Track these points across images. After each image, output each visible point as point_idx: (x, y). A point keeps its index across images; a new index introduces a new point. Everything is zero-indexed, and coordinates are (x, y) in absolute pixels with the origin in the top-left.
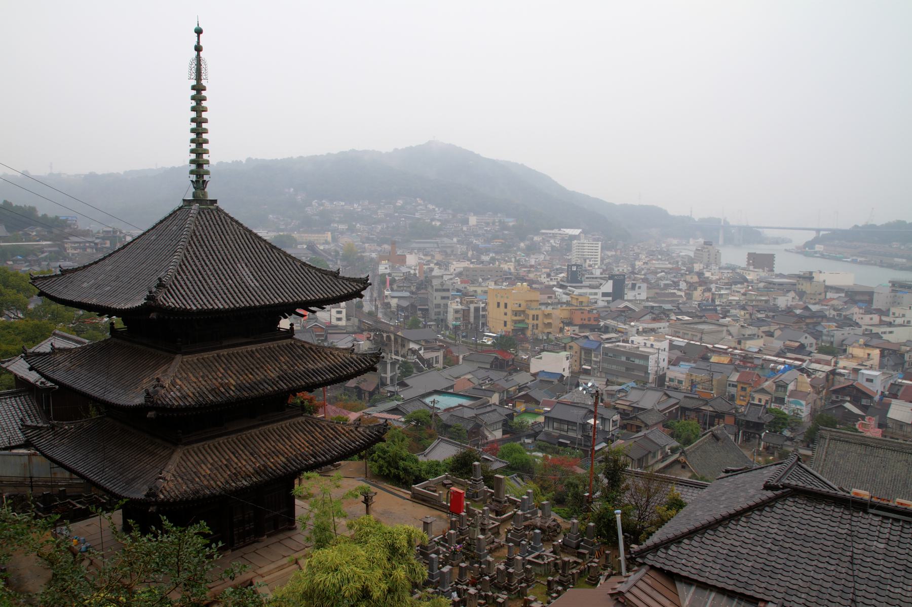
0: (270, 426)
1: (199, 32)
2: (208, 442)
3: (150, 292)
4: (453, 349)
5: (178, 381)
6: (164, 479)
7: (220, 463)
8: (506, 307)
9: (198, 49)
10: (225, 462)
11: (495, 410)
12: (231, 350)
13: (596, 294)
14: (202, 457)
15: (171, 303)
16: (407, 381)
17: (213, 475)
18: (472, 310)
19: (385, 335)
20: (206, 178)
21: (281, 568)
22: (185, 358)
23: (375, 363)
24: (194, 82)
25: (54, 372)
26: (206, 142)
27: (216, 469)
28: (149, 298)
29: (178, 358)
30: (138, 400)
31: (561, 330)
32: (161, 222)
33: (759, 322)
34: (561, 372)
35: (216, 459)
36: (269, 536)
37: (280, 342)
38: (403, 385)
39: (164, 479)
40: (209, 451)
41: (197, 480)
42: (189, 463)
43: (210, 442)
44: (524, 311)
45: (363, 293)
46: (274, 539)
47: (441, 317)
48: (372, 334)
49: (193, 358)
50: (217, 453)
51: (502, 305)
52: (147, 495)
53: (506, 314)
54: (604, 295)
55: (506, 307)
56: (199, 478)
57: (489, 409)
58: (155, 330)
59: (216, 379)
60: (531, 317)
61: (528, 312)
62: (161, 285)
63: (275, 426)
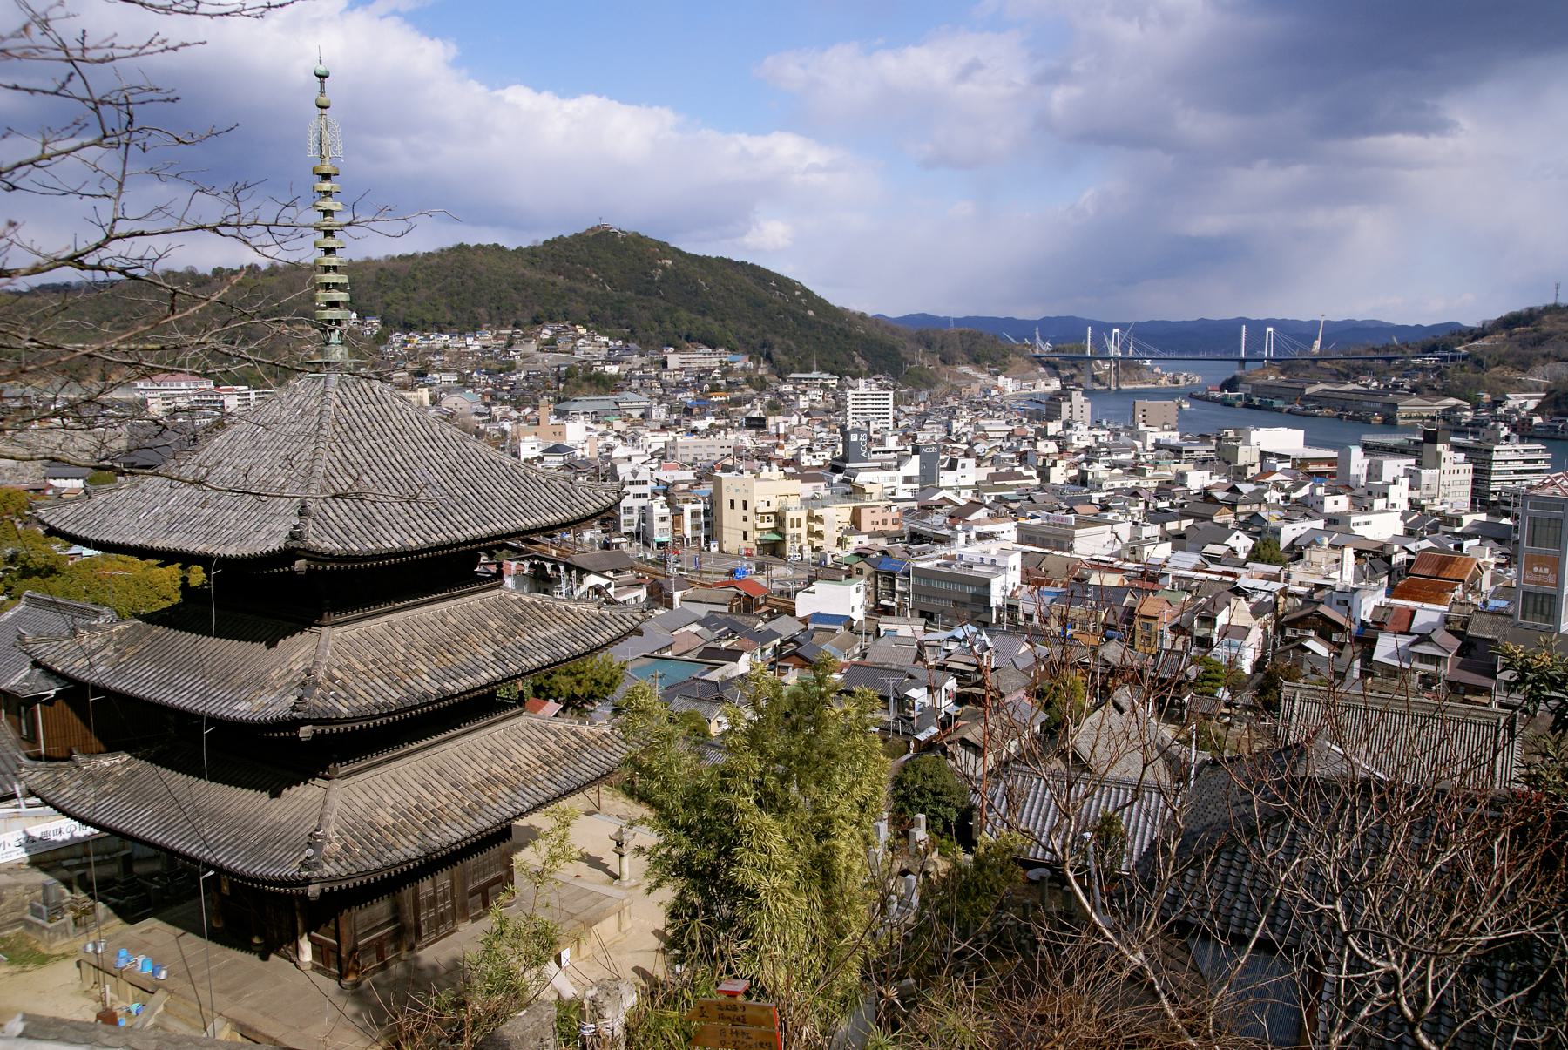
14: (375, 797)
15: (328, 545)
19: (548, 565)
33: (1158, 516)
35: (399, 799)
51: (739, 505)
53: (745, 519)
54: (908, 480)
55: (745, 504)
56: (378, 831)
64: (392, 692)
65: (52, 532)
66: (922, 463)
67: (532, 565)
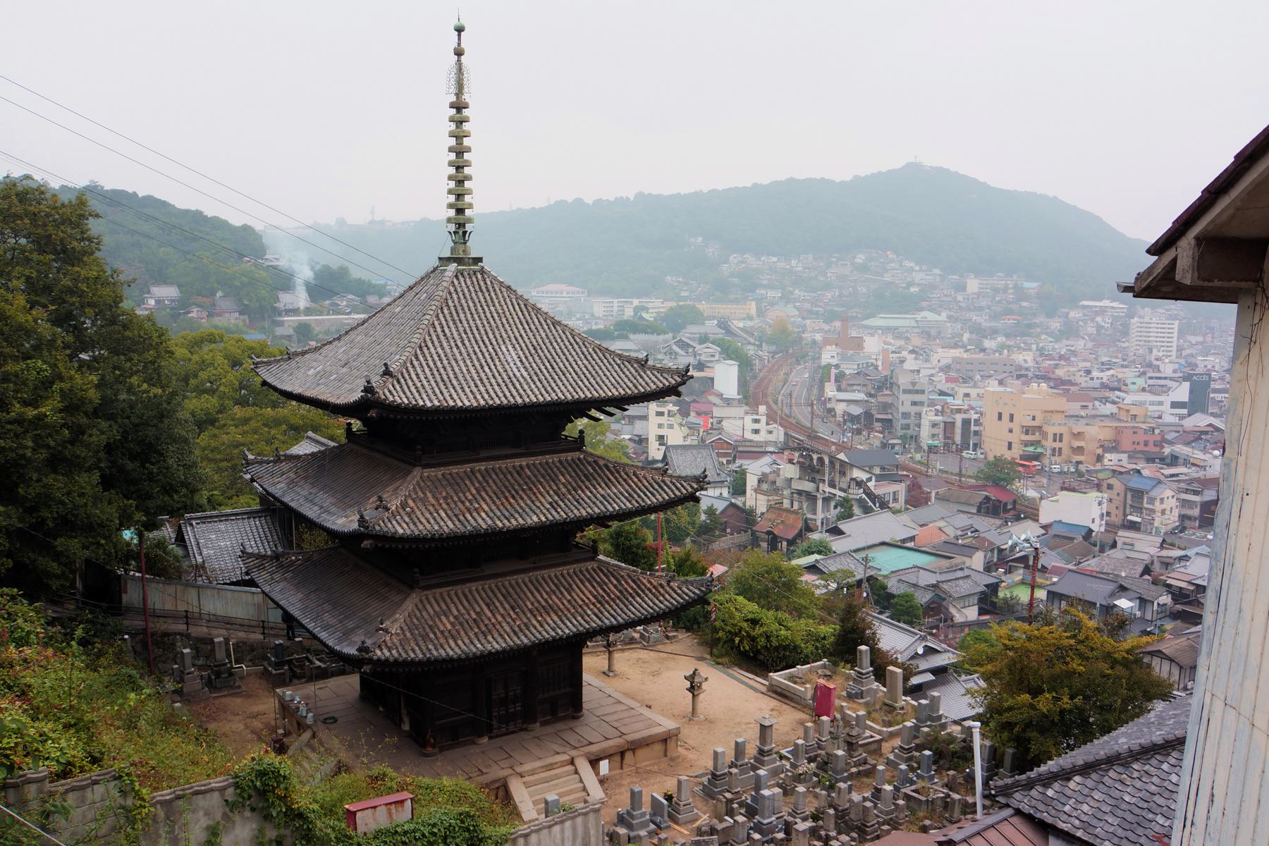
0: (545, 573)
1: (460, 30)
2: (455, 588)
3: (368, 382)
4: (921, 480)
5: (410, 502)
6: (386, 631)
7: (467, 617)
8: (1011, 419)
9: (459, 53)
10: (474, 616)
11: (968, 577)
12: (490, 465)
13: (1160, 403)
14: (444, 607)
16: (843, 526)
17: (454, 632)
18: (959, 424)
19: (815, 457)
20: (468, 227)
21: (550, 767)
22: (426, 472)
23: (697, 490)
24: (453, 99)
25: (274, 484)
26: (469, 178)
27: (461, 624)
28: (369, 389)
29: (417, 472)
30: (345, 522)
31: (1099, 459)
32: (411, 288)
34: (1088, 523)
35: (463, 611)
36: (544, 724)
37: (563, 456)
38: (836, 531)
39: (386, 631)
40: (455, 599)
41: (432, 636)
42: (424, 613)
43: (459, 588)
44: (1040, 428)
45: (680, 389)
46: (549, 729)
47: (910, 432)
48: (797, 454)
49: (438, 472)
50: (466, 604)
51: (1006, 417)
52: (359, 650)
53: (1011, 431)
54: (1175, 405)
55: (1011, 419)
56: (435, 634)
57: (959, 574)
58: (390, 434)
59: (463, 502)
60: (1050, 437)
61: (1045, 428)
62: (387, 373)
63: (552, 572)
64: (449, 523)
65: (265, 383)
66: (1191, 391)
67: (801, 456)
